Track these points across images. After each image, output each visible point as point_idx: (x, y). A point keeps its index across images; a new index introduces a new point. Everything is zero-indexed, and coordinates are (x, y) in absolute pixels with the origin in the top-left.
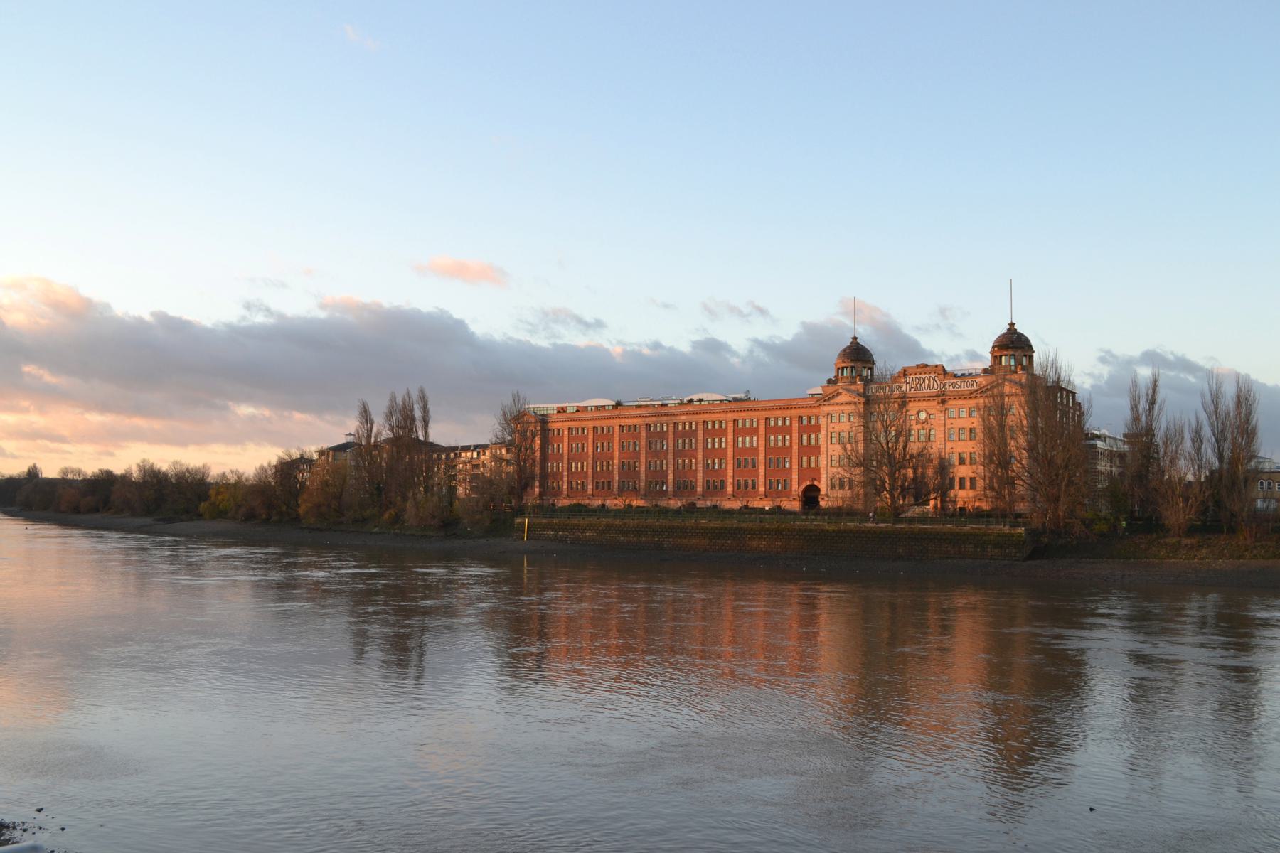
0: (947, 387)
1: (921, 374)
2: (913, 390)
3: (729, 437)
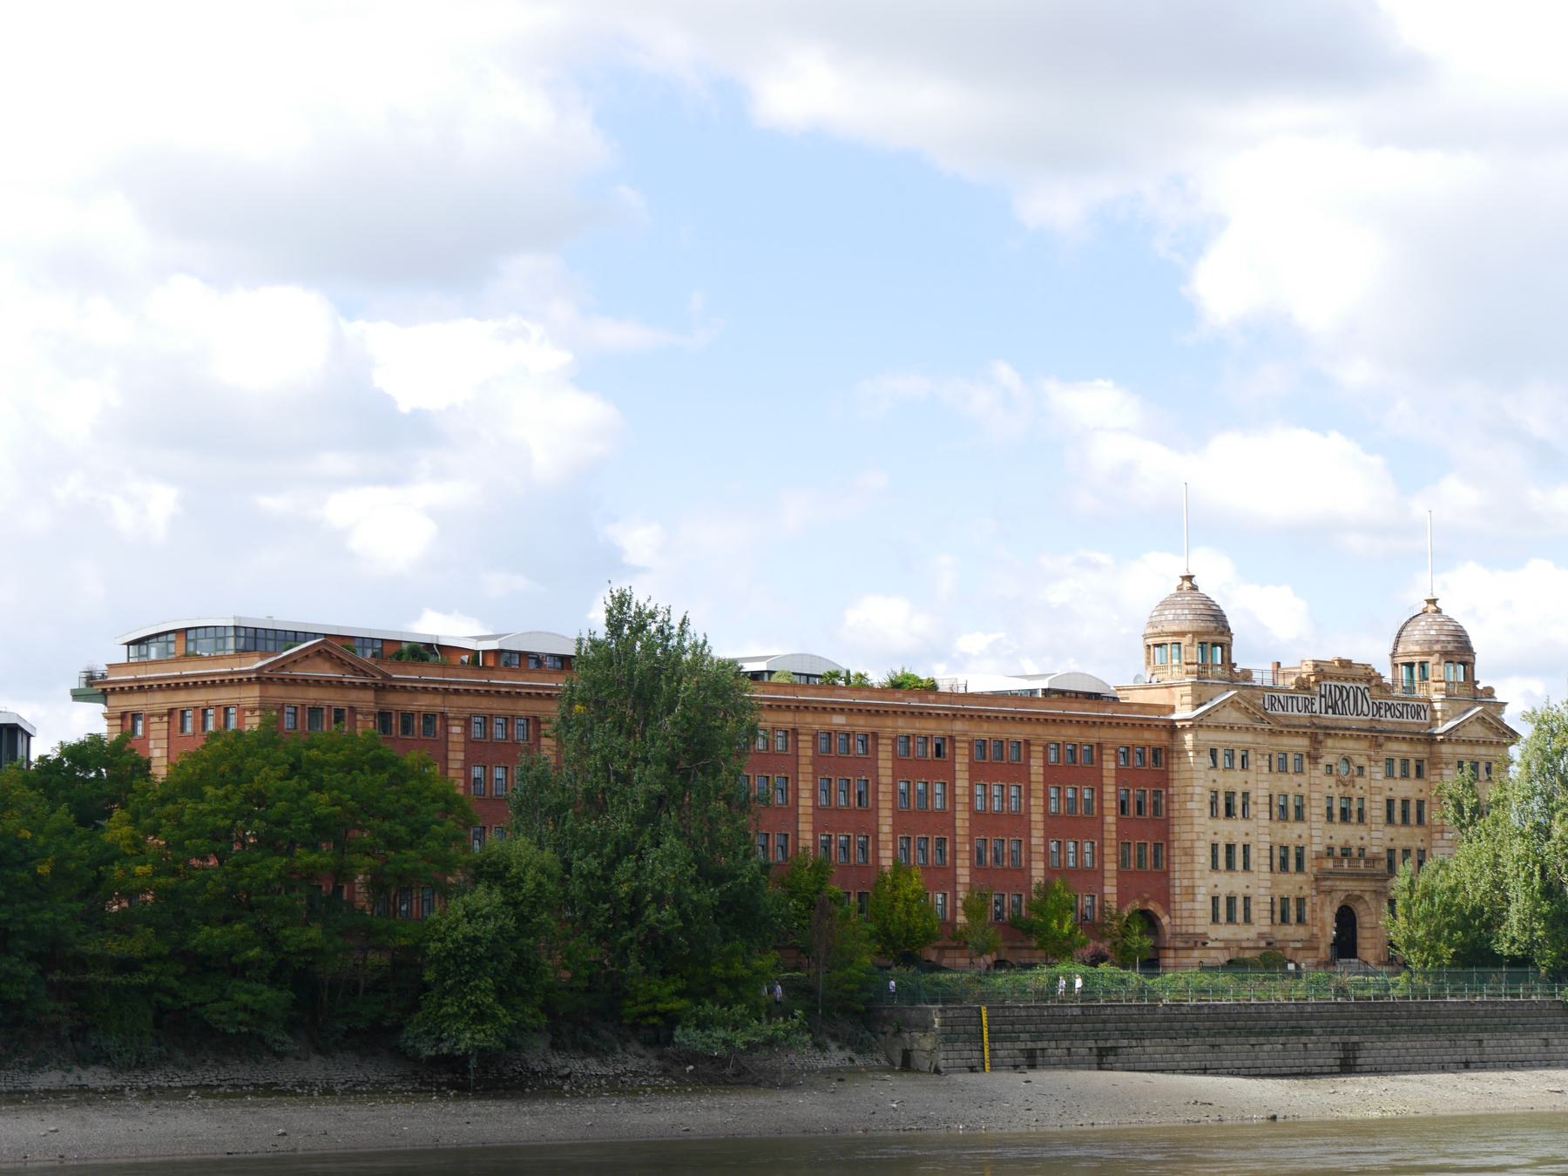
0: (1382, 712)
1: (1346, 680)
3: (959, 783)
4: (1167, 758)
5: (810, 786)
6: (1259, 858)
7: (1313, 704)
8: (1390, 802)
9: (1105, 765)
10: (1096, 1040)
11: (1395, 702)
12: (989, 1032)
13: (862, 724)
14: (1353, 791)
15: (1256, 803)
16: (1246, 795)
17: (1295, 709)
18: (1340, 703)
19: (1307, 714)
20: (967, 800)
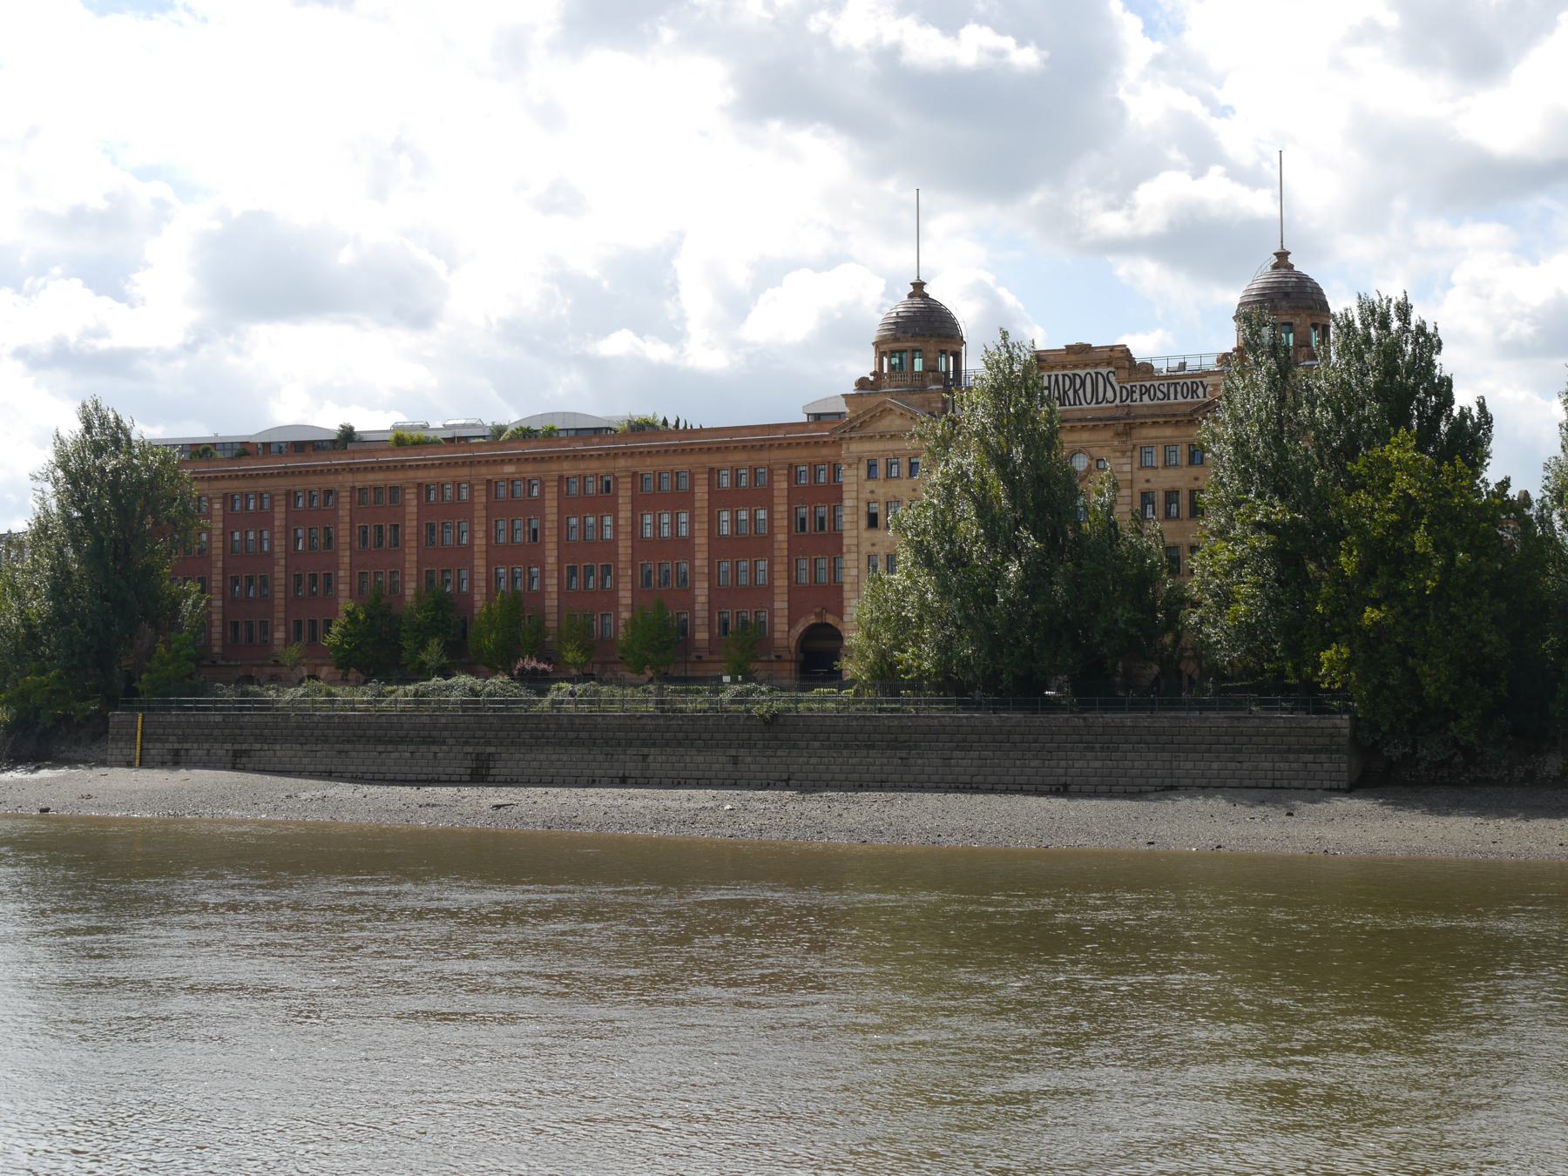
0: (1136, 396)
1: (1076, 367)
3: (621, 514)
5: (484, 528)
9: (776, 485)
10: (233, 744)
11: (1156, 383)
12: (142, 733)
13: (529, 470)
18: (1071, 393)
20: (630, 529)
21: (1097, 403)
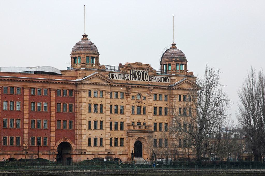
0: (153, 79)
1: (140, 69)
2: (134, 79)
4: (74, 94)
6: (106, 126)
7: (127, 77)
8: (155, 108)
11: (158, 77)
14: (142, 104)
15: (105, 108)
16: (102, 105)
17: (121, 78)
18: (137, 76)
19: (125, 80)
21: (144, 80)
